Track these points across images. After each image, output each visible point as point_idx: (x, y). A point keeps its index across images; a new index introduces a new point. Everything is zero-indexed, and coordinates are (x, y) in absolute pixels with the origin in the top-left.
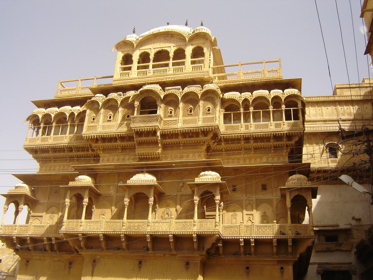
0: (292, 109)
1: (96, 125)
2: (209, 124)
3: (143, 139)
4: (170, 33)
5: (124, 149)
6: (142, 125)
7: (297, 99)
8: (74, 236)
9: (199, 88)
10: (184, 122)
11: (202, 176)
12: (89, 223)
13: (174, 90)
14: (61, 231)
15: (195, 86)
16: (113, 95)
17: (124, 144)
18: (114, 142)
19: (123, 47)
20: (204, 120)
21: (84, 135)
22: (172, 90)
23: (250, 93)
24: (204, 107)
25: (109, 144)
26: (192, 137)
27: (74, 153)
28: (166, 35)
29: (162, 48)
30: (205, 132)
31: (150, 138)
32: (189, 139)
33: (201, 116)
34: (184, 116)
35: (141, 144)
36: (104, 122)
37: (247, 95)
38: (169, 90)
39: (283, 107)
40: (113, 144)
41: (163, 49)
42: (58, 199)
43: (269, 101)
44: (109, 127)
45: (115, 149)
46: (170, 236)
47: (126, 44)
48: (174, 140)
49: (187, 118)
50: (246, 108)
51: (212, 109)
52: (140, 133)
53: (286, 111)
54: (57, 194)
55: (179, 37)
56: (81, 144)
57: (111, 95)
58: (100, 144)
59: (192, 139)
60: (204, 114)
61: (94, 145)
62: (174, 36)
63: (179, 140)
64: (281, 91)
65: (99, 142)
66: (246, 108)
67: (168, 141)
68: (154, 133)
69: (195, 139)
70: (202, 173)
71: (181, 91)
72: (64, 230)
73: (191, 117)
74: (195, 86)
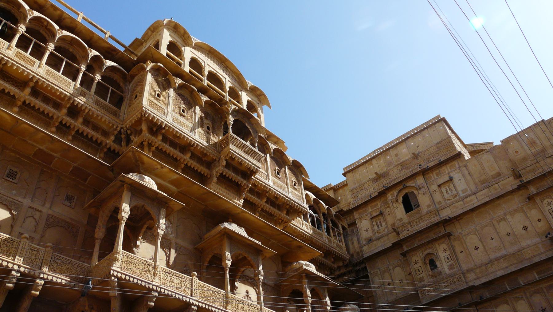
4: (226, 63)
12: (169, 275)
14: (114, 270)
17: (194, 164)
18: (180, 151)
19: (171, 31)
21: (145, 108)
27: (78, 124)
28: (220, 62)
29: (218, 72)
31: (239, 179)
41: (218, 74)
42: (14, 192)
47: (175, 30)
54: (14, 181)
55: (233, 74)
56: (107, 117)
62: (228, 70)
63: (261, 203)
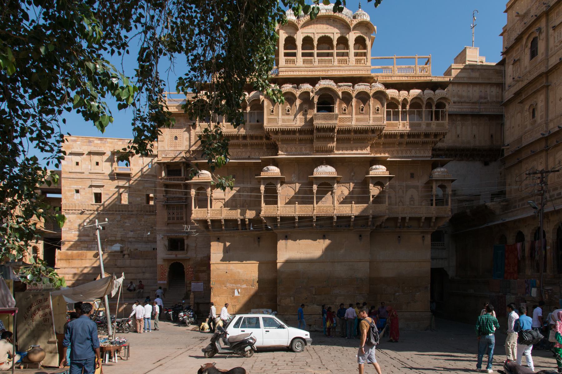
0: (440, 110)
1: (277, 117)
2: (379, 123)
3: (322, 134)
5: (301, 140)
6: (323, 122)
7: (446, 101)
8: (273, 219)
9: (369, 87)
10: (357, 120)
11: (375, 169)
13: (346, 87)
15: (365, 85)
16: (287, 88)
20: (374, 119)
22: (344, 87)
23: (406, 92)
24: (373, 106)
25: (288, 136)
26: (363, 133)
30: (373, 131)
32: (359, 135)
33: (371, 116)
34: (356, 114)
35: (318, 138)
36: (283, 115)
37: (404, 93)
38: (342, 86)
39: (434, 109)
40: (291, 136)
43: (422, 102)
44: (288, 120)
45: (294, 140)
46: (352, 217)
48: (346, 136)
49: (359, 116)
50: (404, 106)
51: (381, 109)
52: (319, 130)
53: (435, 111)
57: (286, 87)
58: (280, 136)
59: (362, 135)
60: (373, 114)
61: (273, 136)
64: (432, 92)
65: (280, 134)
66: (404, 106)
67: (341, 136)
68: (332, 129)
69: (364, 135)
70: (374, 167)
71: (351, 88)
72: (263, 214)
73: (362, 116)
74: (365, 85)
